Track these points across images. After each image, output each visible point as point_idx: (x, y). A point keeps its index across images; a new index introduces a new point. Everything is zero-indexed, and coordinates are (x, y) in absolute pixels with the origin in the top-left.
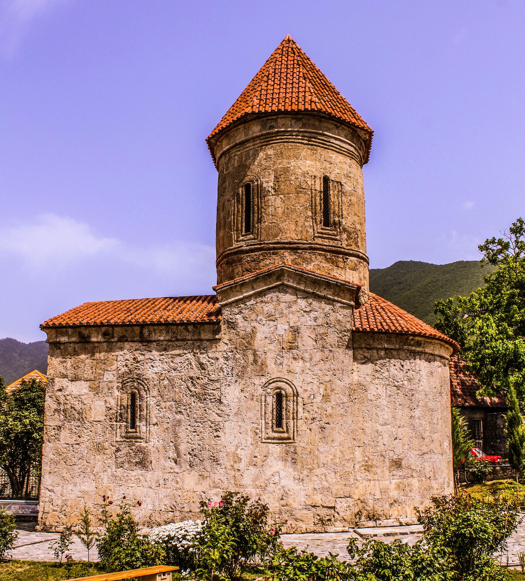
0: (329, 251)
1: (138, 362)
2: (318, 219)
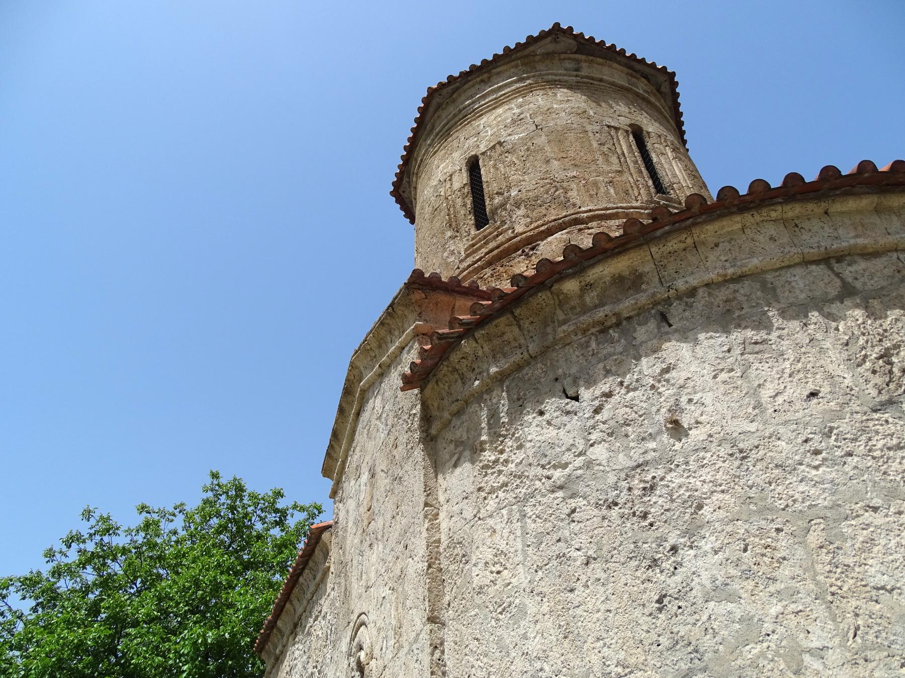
0: (489, 264)
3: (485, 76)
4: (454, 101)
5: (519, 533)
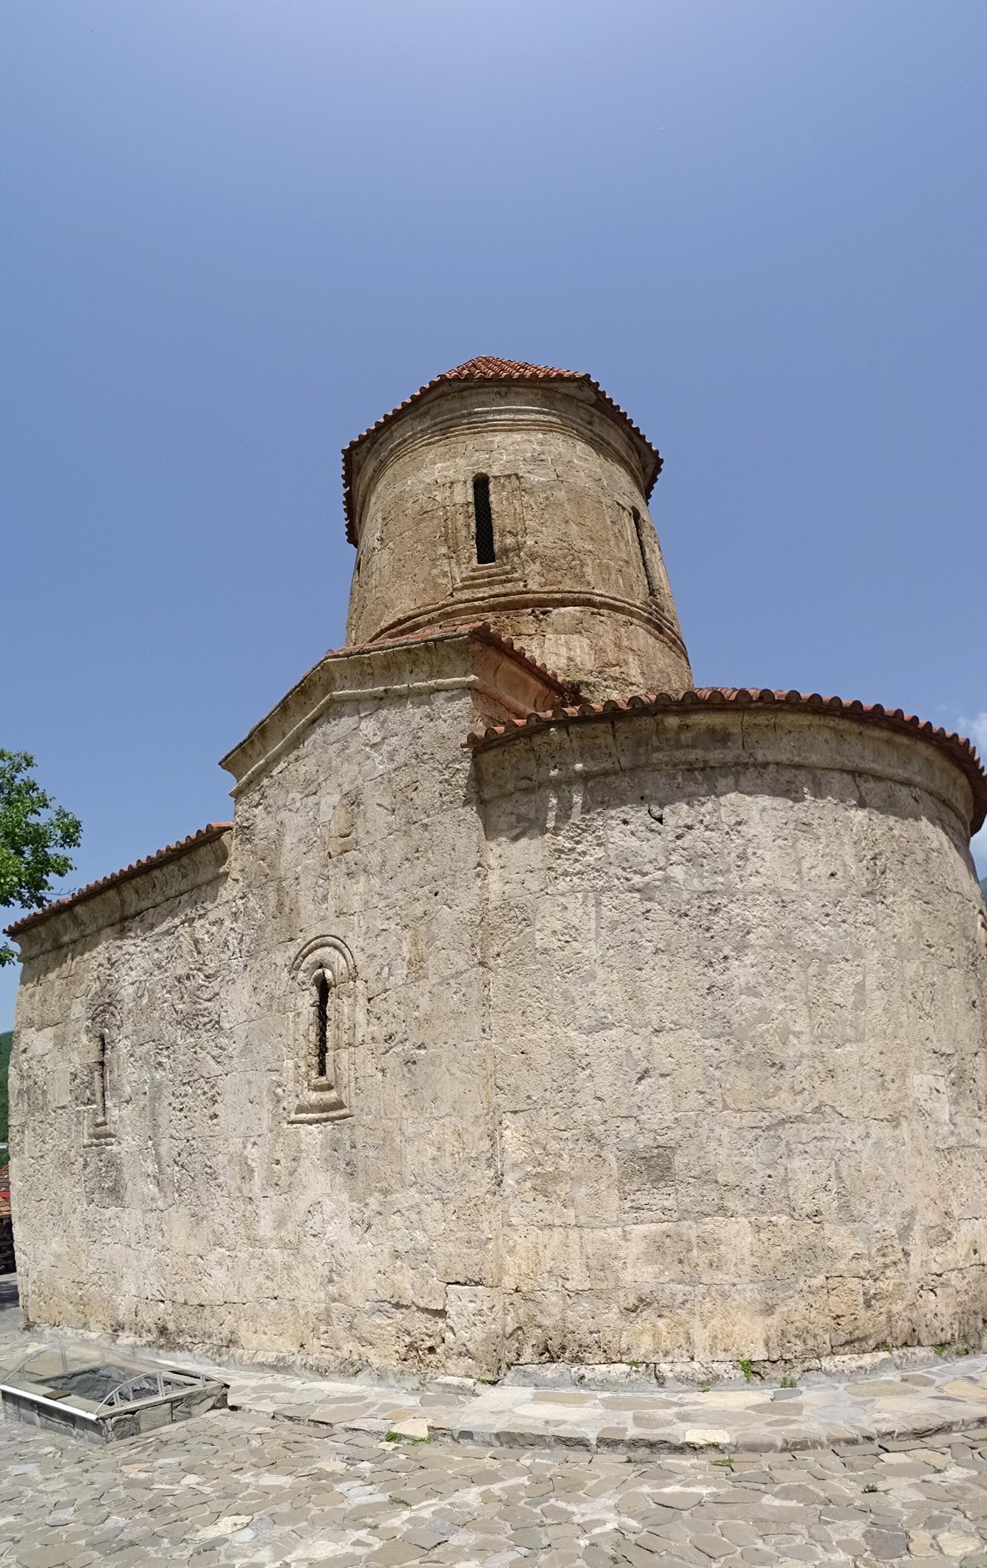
5: (593, 915)
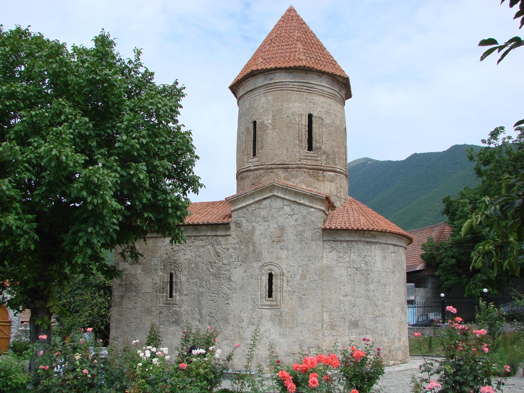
0: (312, 169)
1: (174, 251)
2: (304, 146)
3: (321, 74)
4: (306, 73)
